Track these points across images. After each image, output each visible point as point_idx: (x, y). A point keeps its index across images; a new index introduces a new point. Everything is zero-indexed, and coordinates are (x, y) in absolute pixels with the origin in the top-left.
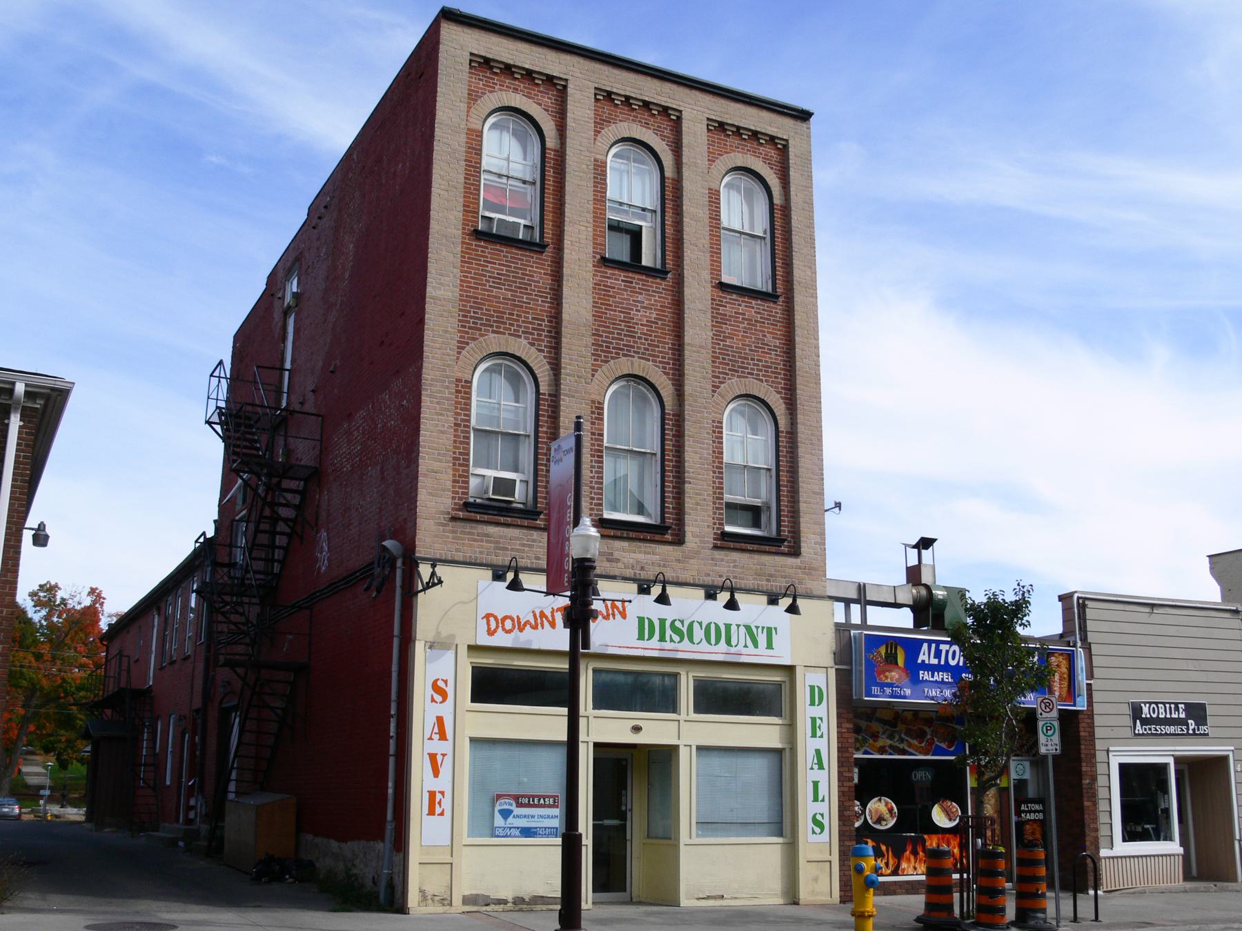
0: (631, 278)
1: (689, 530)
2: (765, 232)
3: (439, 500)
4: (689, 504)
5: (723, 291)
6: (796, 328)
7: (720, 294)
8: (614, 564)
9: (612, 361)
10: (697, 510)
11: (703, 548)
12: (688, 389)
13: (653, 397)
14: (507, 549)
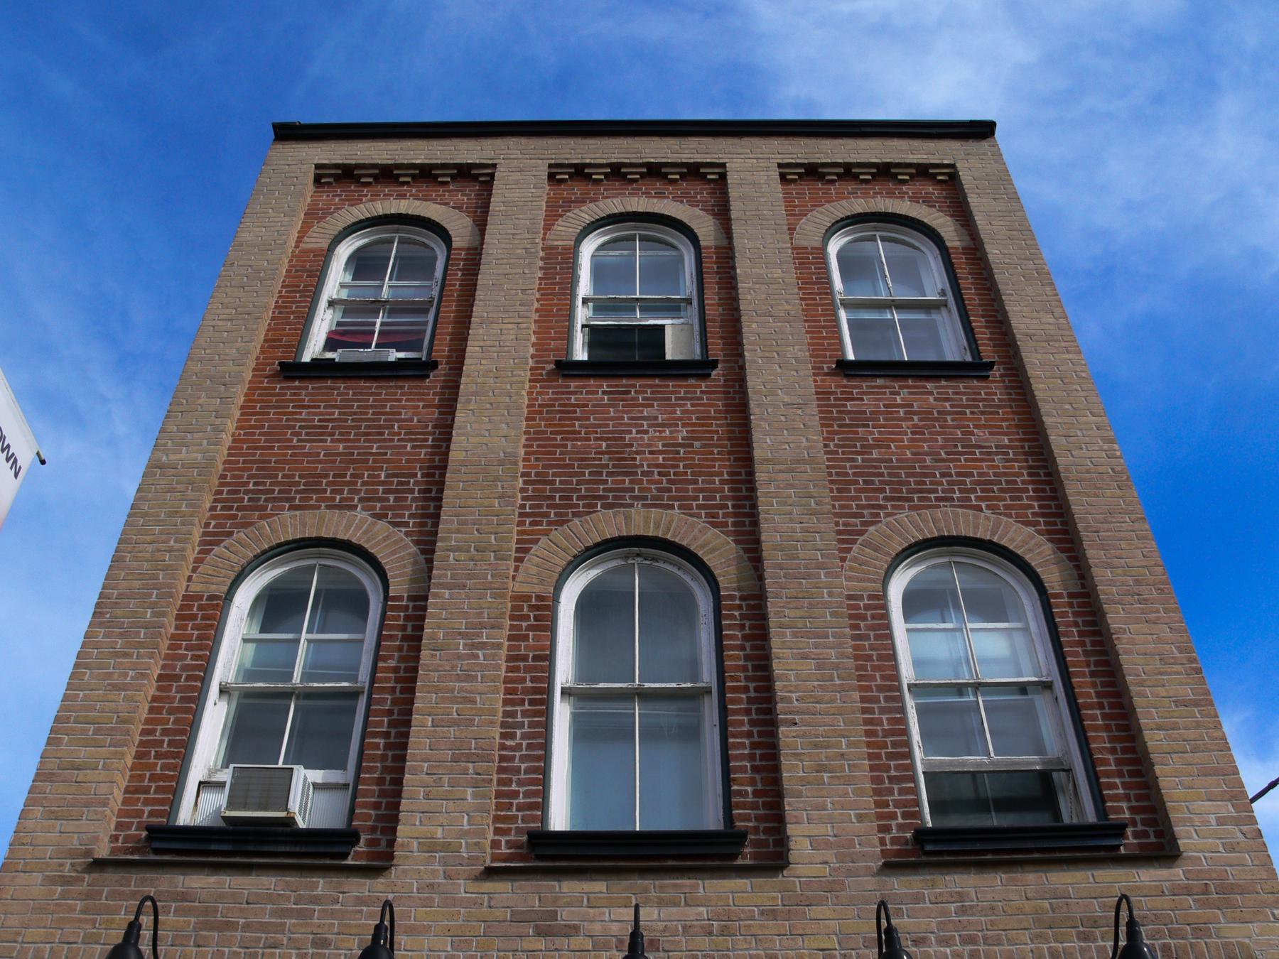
0: (626, 386)
1: (800, 834)
2: (943, 293)
3: (71, 826)
4: (792, 771)
5: (848, 376)
6: (1040, 404)
7: (845, 382)
8: (561, 942)
9: (576, 521)
10: (820, 782)
11: (849, 873)
12: (769, 538)
13: (694, 579)
14: (231, 926)
